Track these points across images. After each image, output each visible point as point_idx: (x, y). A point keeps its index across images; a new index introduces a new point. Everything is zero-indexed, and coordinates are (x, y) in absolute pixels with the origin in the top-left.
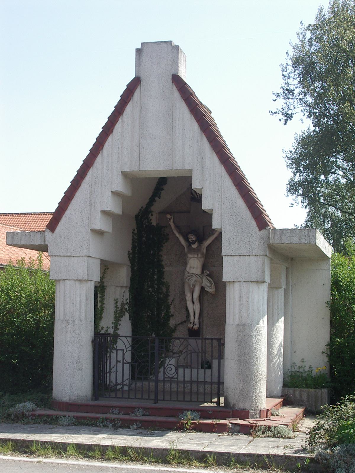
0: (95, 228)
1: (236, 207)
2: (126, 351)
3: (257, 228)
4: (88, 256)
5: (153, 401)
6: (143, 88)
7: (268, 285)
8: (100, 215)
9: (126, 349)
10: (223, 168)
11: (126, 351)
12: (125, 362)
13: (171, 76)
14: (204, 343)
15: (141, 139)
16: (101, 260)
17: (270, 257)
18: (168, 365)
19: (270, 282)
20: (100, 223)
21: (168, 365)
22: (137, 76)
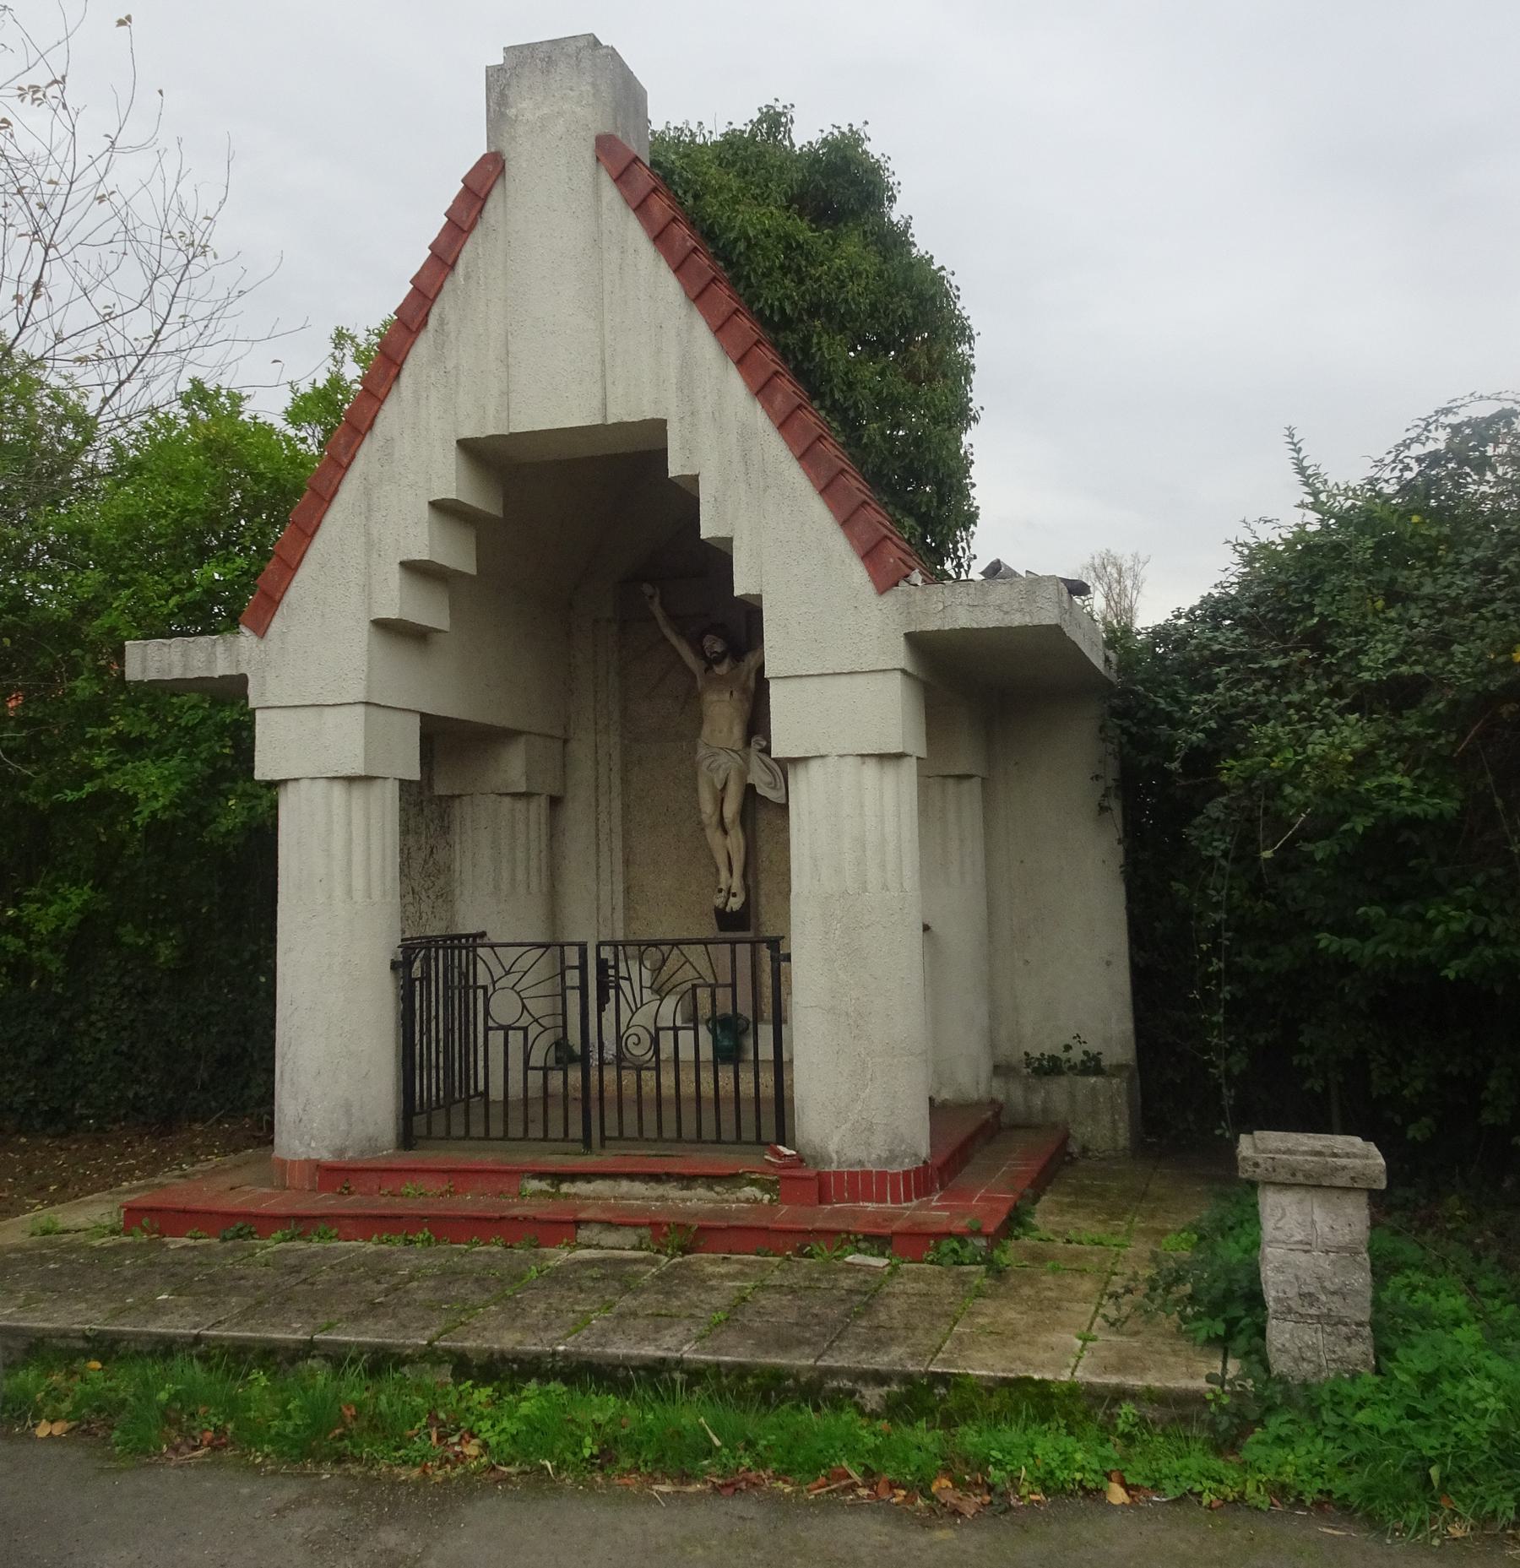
0: (384, 615)
1: (803, 524)
2: (495, 991)
3: (870, 588)
4: (367, 703)
5: (580, 1147)
6: (510, 185)
7: (918, 765)
8: (397, 576)
9: (494, 983)
10: (759, 406)
11: (495, 991)
12: (491, 1023)
13: (593, 141)
14: (471, 955)
15: (510, 338)
16: (423, 716)
17: (920, 676)
18: (628, 1028)
19: (923, 754)
20: (394, 600)
21: (628, 1028)
22: (493, 150)
